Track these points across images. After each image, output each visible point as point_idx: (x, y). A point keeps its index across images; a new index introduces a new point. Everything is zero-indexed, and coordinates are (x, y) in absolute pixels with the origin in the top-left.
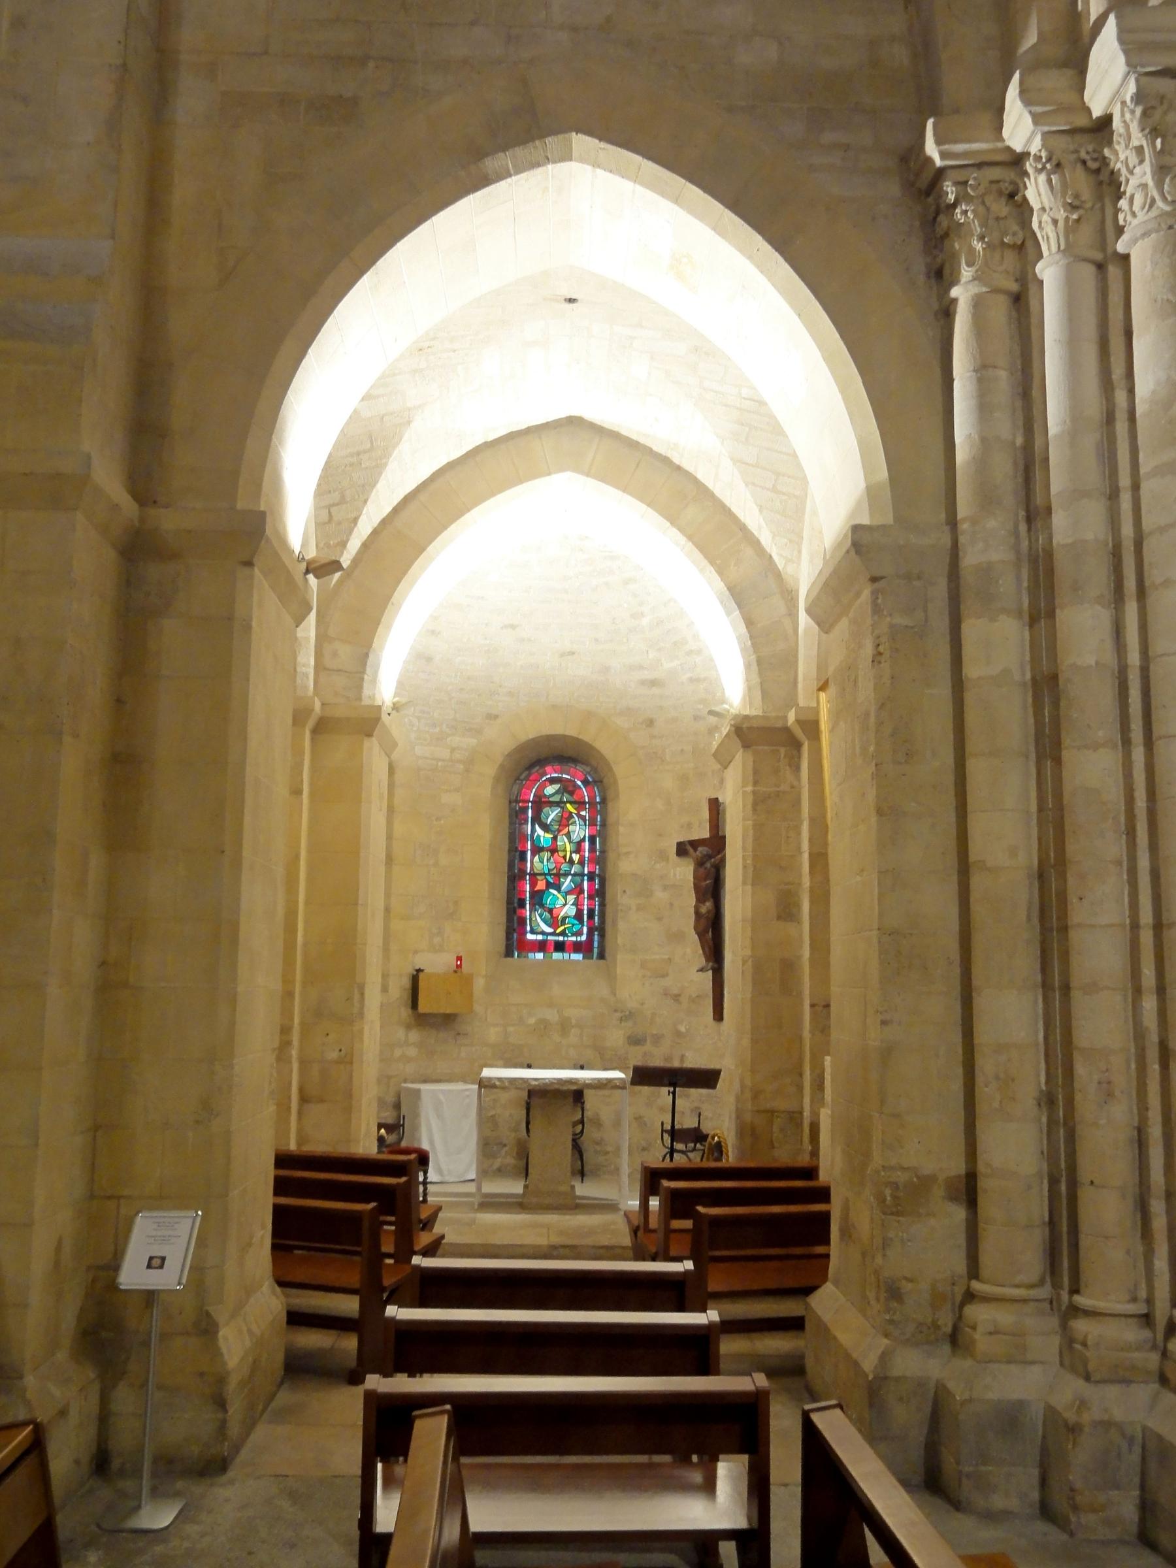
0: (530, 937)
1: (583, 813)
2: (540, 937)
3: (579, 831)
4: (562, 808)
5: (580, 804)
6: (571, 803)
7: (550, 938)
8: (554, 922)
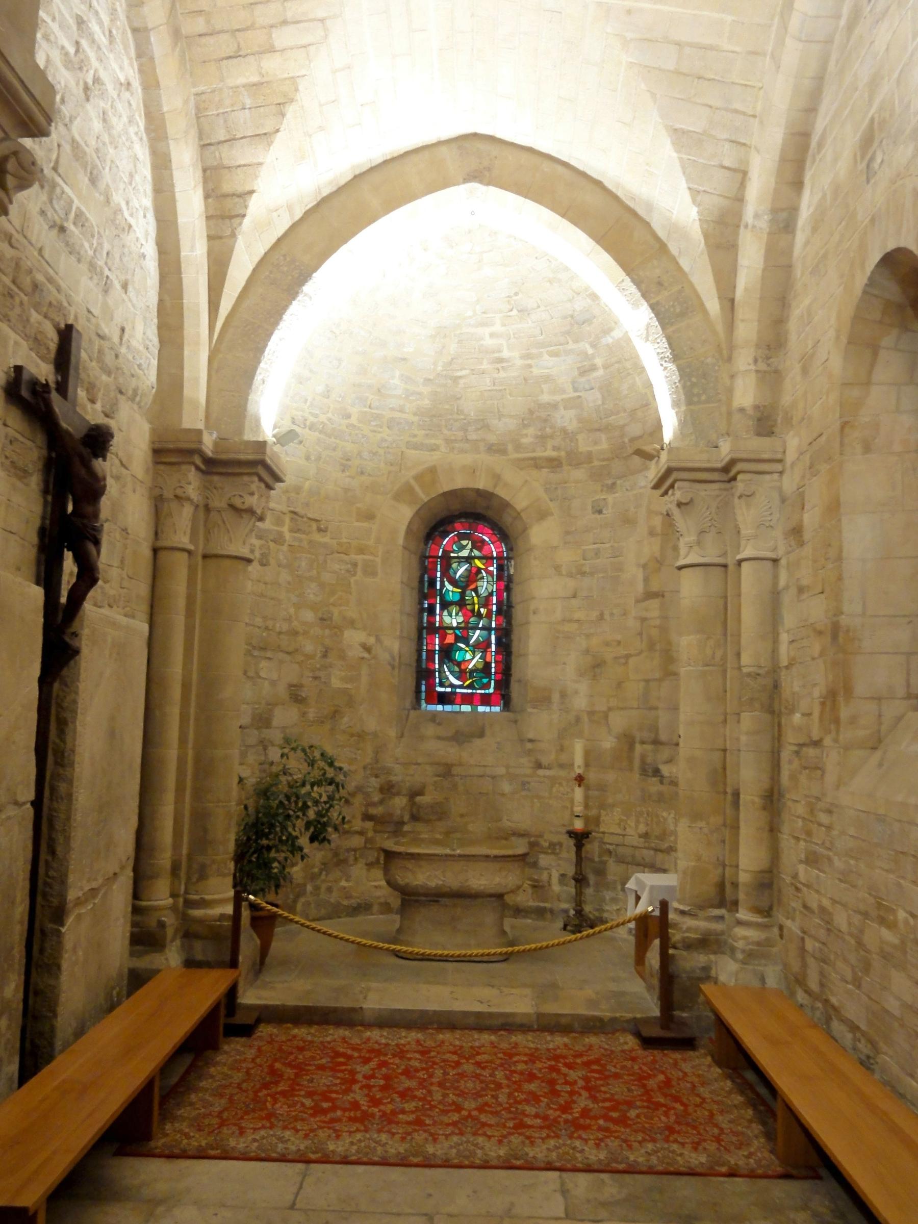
0: (439, 689)
1: (491, 569)
2: (449, 690)
3: (485, 586)
4: (471, 564)
5: (488, 559)
6: (479, 558)
7: (458, 690)
8: (461, 675)
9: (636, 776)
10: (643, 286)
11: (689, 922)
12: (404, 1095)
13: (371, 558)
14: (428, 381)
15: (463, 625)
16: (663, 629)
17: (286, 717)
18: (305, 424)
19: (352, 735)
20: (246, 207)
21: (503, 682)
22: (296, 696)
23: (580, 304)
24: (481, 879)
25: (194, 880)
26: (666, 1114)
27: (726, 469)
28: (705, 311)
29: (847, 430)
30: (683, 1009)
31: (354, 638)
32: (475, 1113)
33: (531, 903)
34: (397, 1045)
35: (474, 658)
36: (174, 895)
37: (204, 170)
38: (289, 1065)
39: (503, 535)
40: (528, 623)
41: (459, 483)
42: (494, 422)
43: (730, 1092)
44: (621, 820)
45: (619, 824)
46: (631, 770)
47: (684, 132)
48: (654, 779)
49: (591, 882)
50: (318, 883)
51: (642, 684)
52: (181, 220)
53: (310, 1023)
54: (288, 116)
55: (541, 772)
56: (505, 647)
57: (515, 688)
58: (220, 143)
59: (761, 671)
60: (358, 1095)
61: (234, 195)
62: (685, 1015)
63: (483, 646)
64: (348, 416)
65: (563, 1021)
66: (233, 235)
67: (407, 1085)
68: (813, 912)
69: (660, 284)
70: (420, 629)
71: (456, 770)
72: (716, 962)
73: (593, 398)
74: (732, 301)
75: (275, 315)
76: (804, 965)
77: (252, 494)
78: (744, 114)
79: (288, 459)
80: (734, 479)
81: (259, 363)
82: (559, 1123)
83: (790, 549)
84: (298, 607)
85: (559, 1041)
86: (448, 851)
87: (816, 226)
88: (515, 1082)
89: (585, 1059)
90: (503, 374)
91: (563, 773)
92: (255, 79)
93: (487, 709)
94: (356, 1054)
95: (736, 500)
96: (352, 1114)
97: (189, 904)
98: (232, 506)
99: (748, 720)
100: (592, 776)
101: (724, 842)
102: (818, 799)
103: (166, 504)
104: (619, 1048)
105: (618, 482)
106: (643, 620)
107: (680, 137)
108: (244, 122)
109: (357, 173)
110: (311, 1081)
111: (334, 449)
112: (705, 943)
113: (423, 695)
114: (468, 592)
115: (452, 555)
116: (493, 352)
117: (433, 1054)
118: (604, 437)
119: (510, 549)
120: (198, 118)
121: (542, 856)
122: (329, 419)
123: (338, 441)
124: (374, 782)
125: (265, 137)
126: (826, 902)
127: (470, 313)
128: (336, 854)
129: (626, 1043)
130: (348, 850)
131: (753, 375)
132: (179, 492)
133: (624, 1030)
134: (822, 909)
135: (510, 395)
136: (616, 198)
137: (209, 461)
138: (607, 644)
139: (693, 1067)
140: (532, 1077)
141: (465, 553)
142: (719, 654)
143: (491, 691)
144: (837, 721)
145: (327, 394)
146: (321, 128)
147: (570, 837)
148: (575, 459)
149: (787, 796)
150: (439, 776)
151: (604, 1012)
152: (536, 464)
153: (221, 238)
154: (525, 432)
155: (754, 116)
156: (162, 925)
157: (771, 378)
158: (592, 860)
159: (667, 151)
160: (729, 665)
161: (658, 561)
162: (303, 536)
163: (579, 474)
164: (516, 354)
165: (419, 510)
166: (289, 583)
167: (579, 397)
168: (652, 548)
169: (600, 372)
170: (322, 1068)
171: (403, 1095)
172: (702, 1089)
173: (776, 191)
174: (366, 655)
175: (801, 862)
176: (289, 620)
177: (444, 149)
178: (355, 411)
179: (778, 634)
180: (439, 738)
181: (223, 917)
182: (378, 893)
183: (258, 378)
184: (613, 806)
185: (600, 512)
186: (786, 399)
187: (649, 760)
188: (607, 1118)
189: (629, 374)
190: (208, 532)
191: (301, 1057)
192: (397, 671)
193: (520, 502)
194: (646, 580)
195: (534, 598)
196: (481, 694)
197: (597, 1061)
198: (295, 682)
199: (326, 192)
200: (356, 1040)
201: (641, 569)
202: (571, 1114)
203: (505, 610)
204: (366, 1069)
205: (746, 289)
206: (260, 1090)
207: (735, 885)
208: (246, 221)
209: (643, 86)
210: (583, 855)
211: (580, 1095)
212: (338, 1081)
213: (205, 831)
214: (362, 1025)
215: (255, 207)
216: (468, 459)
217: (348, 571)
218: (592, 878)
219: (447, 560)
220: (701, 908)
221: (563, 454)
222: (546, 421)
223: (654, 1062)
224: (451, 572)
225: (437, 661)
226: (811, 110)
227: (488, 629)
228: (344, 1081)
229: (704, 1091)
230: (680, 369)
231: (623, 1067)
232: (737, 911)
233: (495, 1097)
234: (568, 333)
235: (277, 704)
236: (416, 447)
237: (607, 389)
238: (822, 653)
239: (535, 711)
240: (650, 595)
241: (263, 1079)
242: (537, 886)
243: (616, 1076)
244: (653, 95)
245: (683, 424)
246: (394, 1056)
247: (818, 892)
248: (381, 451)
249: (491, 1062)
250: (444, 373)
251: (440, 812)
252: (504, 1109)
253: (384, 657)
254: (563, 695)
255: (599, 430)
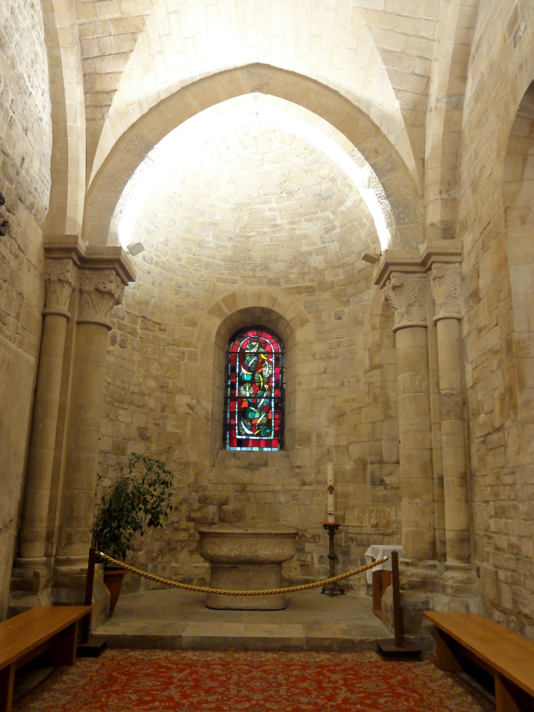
0: (238, 437)
1: (271, 360)
2: (244, 437)
3: (267, 371)
4: (258, 357)
5: (269, 354)
6: (263, 353)
7: (250, 438)
9: (369, 486)
10: (366, 153)
11: (411, 570)
12: (208, 691)
13: (194, 349)
14: (230, 239)
15: (253, 395)
16: (383, 388)
17: (137, 448)
18: (152, 261)
19: (180, 464)
20: (111, 100)
21: (280, 432)
22: (143, 435)
23: (324, 186)
24: (266, 550)
25: (63, 545)
26: (407, 700)
27: (423, 263)
28: (406, 168)
29: (508, 212)
30: (410, 633)
31: (182, 400)
32: (261, 702)
33: (300, 577)
34: (205, 661)
35: (260, 416)
36: (47, 555)
37: (85, 76)
38: (124, 674)
39: (279, 339)
40: (295, 391)
41: (250, 304)
42: (272, 265)
43: (452, 686)
44: (359, 517)
45: (358, 520)
46: (365, 482)
47: (389, 52)
48: (381, 487)
49: (340, 561)
50: (156, 563)
51: (370, 425)
52: (67, 102)
53: (142, 648)
54: (139, 41)
55: (305, 488)
56: (280, 409)
57: (287, 435)
58: (94, 57)
59: (455, 392)
60: (173, 692)
61: (103, 92)
62: (412, 637)
63: (266, 409)
64: (180, 260)
65: (326, 643)
66: (103, 118)
67: (210, 685)
68: (504, 550)
69: (377, 152)
70: (226, 398)
71: (249, 488)
72: (432, 599)
73: (334, 247)
74: (423, 160)
75: (129, 171)
76: (499, 592)
77: (111, 282)
78: (427, 39)
79: (137, 263)
80: (430, 269)
81: (118, 199)
82: (326, 708)
83: (469, 309)
84: (145, 377)
85: (323, 657)
86: (243, 531)
87: (477, 98)
88: (292, 682)
89: (342, 667)
90: (277, 234)
91: (320, 488)
92: (117, 15)
93: (270, 449)
94: (174, 667)
95: (432, 282)
96: (167, 704)
97: (58, 562)
98: (97, 290)
99: (447, 425)
100: (339, 488)
101: (433, 512)
102: (503, 467)
103: (52, 285)
104: (367, 661)
105: (351, 299)
106: (370, 384)
107: (388, 55)
108: (110, 44)
109: (184, 85)
110: (139, 683)
111: (171, 280)
112: (425, 584)
113: (228, 441)
114: (256, 375)
115: (246, 351)
116: (271, 220)
117: (231, 666)
118: (341, 271)
119: (283, 348)
120: (80, 41)
121: (307, 544)
122: (168, 260)
123: (173, 275)
124: (195, 496)
125: (124, 55)
126: (514, 540)
127: (256, 195)
128: (169, 544)
129: (371, 657)
130: (177, 542)
131: (439, 201)
132: (62, 277)
133: (369, 649)
134: (512, 546)
135: (282, 247)
136: (347, 101)
137: (83, 259)
138: (347, 402)
139: (422, 671)
140: (304, 679)
141: (254, 350)
142: (424, 384)
143: (272, 437)
144: (515, 407)
145: (166, 243)
146: (160, 52)
147: (326, 529)
148: (323, 287)
149: (478, 474)
150: (237, 492)
151: (356, 636)
152: (299, 291)
153: (94, 120)
154: (291, 271)
155: (434, 40)
156: (37, 575)
157: (451, 202)
158: (341, 546)
159: (380, 65)
160: (431, 391)
161: (378, 345)
162: (150, 333)
163: (326, 296)
164: (285, 221)
165: (225, 320)
166: (140, 361)
167: (325, 247)
168: (374, 337)
169: (338, 230)
170: (148, 675)
171: (208, 691)
172: (431, 685)
173: (450, 83)
174: (190, 412)
175: (491, 517)
176: (139, 385)
177: (239, 73)
178: (184, 257)
179: (464, 367)
180: (238, 467)
181: (82, 570)
182: (198, 572)
183: (117, 209)
184: (354, 507)
185: (340, 318)
186: (462, 214)
187: (377, 474)
188: (362, 704)
189: (356, 229)
190: (81, 307)
191: (133, 669)
192: (210, 422)
193: (289, 315)
194: (371, 358)
195: (299, 375)
196: (265, 440)
197: (352, 668)
198: (142, 426)
199: (163, 97)
200: (175, 658)
201: (368, 352)
202: (335, 701)
203: (280, 386)
204: (181, 675)
205: (432, 148)
206: (99, 689)
207: (443, 543)
208: (111, 109)
209: (363, 22)
210: (335, 542)
211: (341, 689)
212: (159, 683)
213: (72, 509)
214: (180, 649)
215: (118, 101)
216: (256, 289)
217: (179, 357)
218: (340, 558)
219: (243, 355)
220: (420, 559)
221: (315, 283)
222: (304, 263)
223: (394, 668)
224: (246, 362)
225: (237, 419)
226: (471, 28)
227: (269, 398)
228: (163, 683)
229: (434, 686)
230: (391, 203)
231: (371, 672)
232: (446, 561)
233: (278, 692)
234: (317, 206)
235: (130, 440)
236: (223, 281)
237: (343, 240)
238: (499, 366)
239: (300, 447)
240: (373, 367)
241: (103, 682)
242: (304, 565)
243: (367, 677)
244: (370, 28)
245: (394, 237)
246: (202, 667)
247: (506, 534)
248: (201, 283)
249: (274, 670)
250: (241, 234)
251: (238, 517)
252: (284, 699)
253: (202, 413)
254: (319, 436)
255: (338, 267)
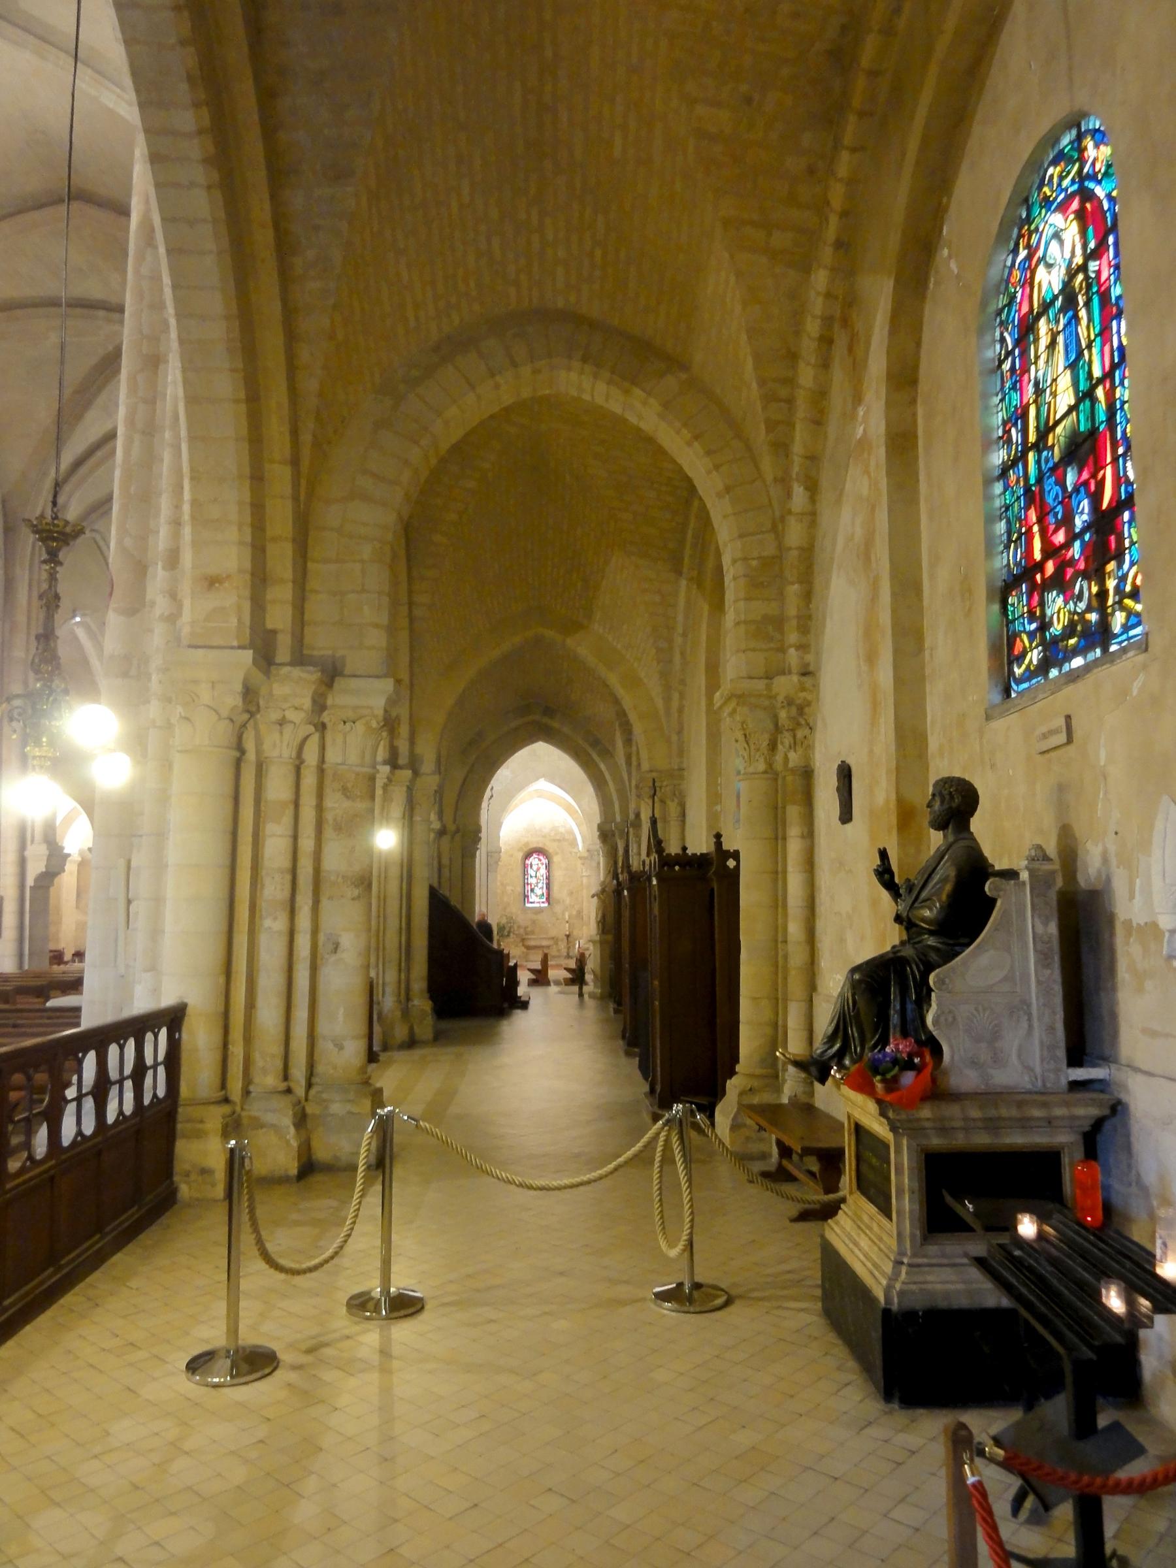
31: (509, 888)
148: (564, 840)
251: (533, 933)
